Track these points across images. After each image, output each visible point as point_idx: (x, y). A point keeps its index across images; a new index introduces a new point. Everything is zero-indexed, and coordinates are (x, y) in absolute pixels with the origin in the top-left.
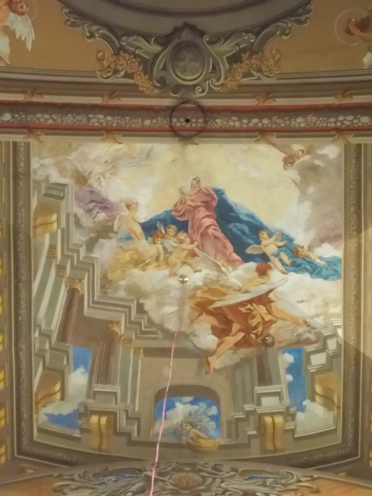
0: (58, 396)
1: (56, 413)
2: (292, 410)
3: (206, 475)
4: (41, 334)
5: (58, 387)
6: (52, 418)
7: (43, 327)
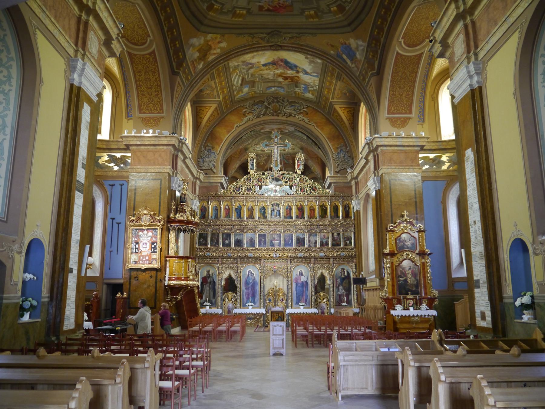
3: (280, 104)
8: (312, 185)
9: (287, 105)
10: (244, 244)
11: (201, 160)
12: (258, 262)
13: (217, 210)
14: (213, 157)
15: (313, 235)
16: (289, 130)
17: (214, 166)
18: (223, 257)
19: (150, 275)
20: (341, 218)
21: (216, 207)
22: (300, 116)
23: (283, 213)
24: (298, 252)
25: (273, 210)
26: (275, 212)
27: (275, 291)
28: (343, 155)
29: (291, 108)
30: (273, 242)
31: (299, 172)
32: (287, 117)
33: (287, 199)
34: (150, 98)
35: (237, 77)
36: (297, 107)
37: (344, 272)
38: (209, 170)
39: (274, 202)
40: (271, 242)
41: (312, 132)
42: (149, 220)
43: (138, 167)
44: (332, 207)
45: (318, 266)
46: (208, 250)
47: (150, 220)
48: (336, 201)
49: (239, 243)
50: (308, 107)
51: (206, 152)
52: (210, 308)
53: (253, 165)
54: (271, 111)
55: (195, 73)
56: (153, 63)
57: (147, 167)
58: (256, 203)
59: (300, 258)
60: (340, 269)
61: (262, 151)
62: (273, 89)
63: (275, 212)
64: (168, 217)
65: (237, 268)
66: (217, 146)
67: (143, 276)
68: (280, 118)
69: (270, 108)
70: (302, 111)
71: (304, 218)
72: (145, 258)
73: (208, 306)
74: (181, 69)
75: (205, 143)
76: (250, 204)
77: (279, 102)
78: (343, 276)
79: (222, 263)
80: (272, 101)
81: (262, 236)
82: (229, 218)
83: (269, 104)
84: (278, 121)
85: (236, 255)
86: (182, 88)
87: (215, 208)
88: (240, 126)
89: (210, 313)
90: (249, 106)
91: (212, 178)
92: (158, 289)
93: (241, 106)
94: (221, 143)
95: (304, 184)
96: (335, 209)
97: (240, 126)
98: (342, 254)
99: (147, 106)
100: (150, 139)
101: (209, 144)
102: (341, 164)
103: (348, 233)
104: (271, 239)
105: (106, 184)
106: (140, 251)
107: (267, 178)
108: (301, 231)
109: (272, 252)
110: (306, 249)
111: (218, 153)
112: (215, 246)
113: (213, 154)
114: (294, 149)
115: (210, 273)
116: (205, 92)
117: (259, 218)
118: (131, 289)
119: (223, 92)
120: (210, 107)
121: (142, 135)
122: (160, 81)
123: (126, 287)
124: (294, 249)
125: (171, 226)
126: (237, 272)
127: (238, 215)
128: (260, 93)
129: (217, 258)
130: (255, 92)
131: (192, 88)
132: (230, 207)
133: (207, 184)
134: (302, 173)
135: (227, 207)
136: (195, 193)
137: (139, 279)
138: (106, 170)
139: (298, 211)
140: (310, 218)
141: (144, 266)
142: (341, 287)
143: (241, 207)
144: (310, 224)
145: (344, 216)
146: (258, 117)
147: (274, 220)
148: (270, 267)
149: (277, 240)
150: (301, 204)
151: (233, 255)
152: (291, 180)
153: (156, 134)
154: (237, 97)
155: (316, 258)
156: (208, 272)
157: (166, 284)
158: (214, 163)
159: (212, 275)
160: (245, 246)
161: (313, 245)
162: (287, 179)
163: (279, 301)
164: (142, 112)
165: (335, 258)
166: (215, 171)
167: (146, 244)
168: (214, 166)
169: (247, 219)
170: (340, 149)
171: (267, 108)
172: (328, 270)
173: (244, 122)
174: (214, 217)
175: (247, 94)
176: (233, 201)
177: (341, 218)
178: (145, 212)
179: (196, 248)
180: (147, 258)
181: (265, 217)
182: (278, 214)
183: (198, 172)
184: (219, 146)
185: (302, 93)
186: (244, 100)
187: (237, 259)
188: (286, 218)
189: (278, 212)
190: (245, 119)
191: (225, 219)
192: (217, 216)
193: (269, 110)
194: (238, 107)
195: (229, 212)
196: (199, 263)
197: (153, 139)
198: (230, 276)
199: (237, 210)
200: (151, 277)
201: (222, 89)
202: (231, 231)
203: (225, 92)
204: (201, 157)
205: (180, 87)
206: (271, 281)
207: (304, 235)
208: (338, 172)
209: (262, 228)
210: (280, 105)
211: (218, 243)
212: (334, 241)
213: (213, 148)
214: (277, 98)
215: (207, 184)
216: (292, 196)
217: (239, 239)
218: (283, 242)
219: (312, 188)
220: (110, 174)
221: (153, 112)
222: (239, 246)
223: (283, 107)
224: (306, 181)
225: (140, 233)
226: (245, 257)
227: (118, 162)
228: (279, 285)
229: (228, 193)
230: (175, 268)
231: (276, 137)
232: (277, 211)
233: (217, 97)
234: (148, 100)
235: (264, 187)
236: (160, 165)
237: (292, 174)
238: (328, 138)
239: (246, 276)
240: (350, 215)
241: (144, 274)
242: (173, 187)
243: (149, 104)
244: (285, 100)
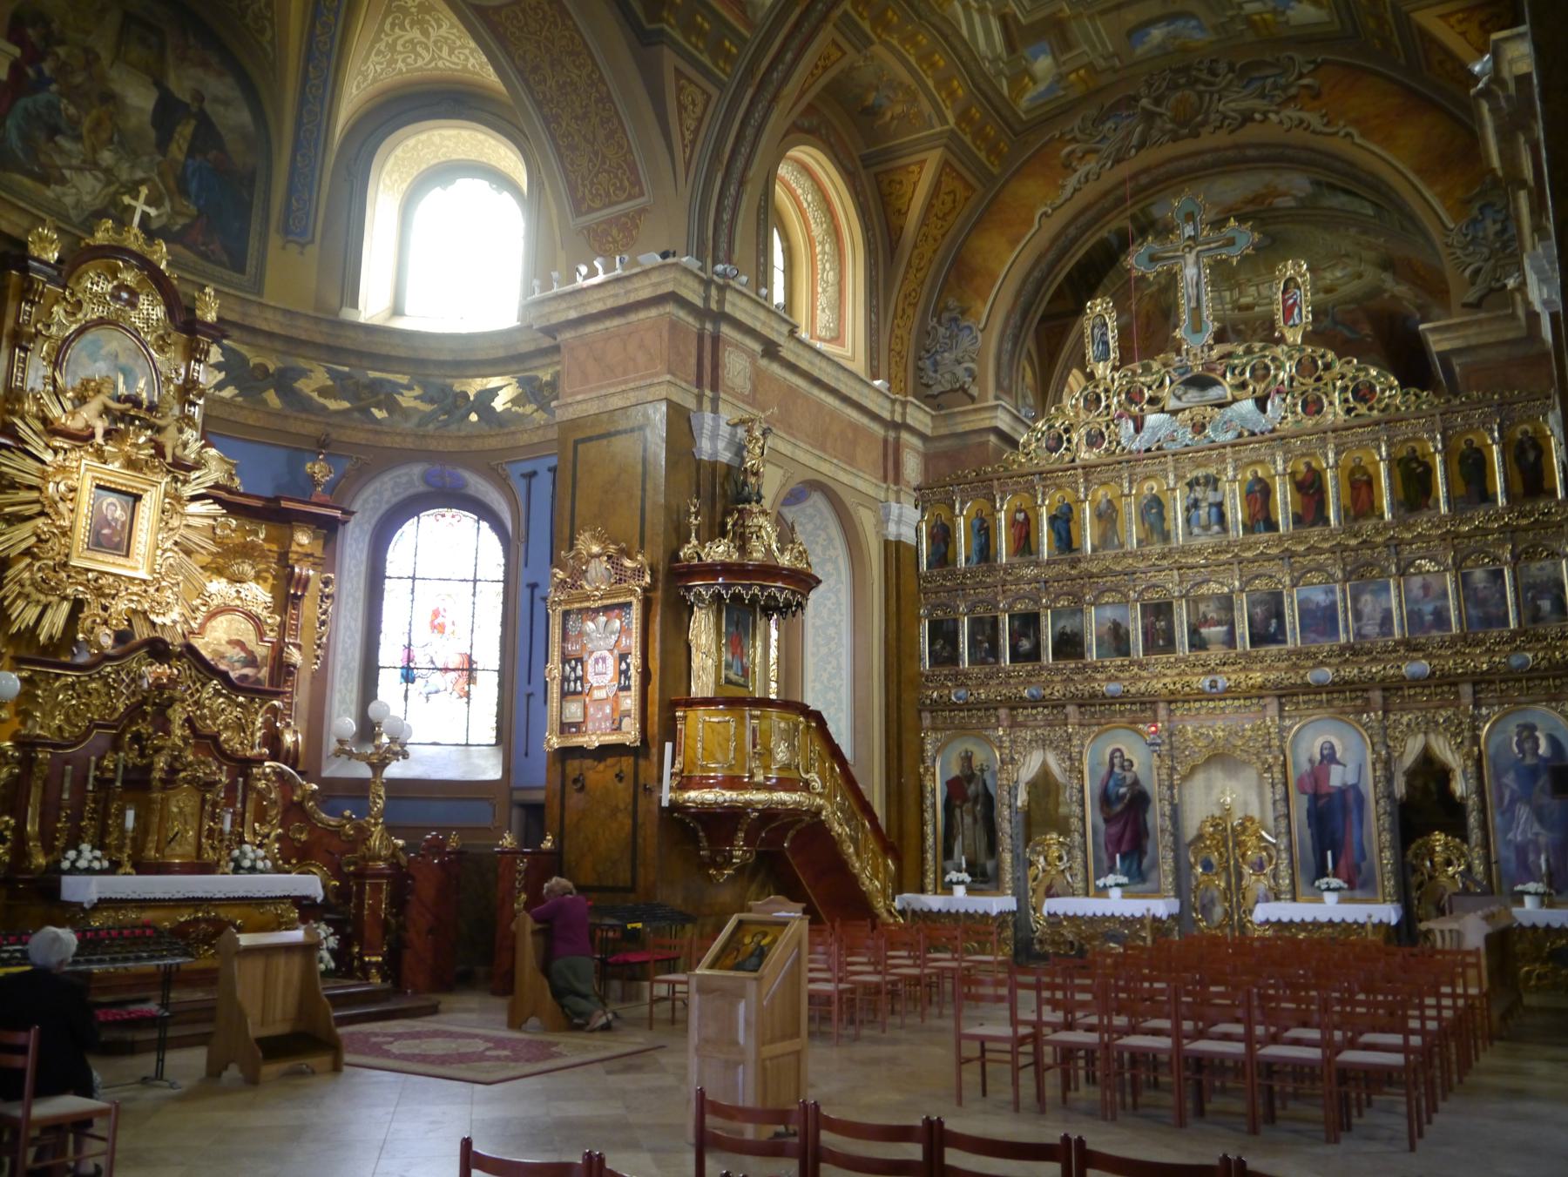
0: (1031, 84)
1: (1035, 94)
2: (1280, 9)
4: (990, 62)
5: (1027, 79)
6: (1033, 99)
7: (990, 56)
8: (1354, 379)
9: (1231, 81)
10: (1090, 650)
11: (928, 362)
12: (1149, 713)
13: (984, 531)
14: (965, 341)
16: (1295, 197)
17: (970, 372)
18: (1015, 704)
19: (617, 770)
20: (1501, 501)
21: (983, 521)
22: (1291, 112)
23: (1236, 512)
24: (1310, 663)
25: (1195, 504)
26: (1203, 512)
27: (1225, 829)
28: (1498, 226)
29: (1245, 92)
30: (1204, 631)
31: (1294, 336)
32: (1232, 132)
33: (1246, 454)
34: (596, 154)
35: (977, 18)
36: (1270, 80)
37: (1536, 741)
38: (955, 391)
39: (1195, 474)
40: (1194, 631)
41: (1352, 164)
42: (606, 573)
43: (579, 397)
44: (1456, 458)
45: (1405, 720)
46: (960, 679)
47: (610, 576)
48: (1471, 429)
49: (1069, 645)
50: (1318, 66)
51: (942, 330)
52: (970, 890)
53: (1106, 343)
54: (1169, 126)
55: (750, 25)
56: (559, 20)
57: (603, 392)
58: (1126, 485)
59: (1318, 689)
60: (1512, 729)
61: (1241, 308)
62: (1157, 34)
63: (1203, 512)
64: (675, 557)
65: (1070, 740)
66: (979, 304)
67: (600, 775)
68: (1207, 140)
69: (1161, 115)
70: (1293, 91)
71: (1326, 521)
72: (602, 709)
73: (958, 883)
74: (665, 14)
75: (939, 296)
76: (1101, 493)
77: (1197, 80)
78: (1529, 761)
79: (1014, 724)
80: (1168, 88)
81: (1159, 611)
82: (1031, 553)
83: (1157, 101)
84: (1208, 158)
85: (1058, 691)
86: (704, 92)
87: (977, 523)
88: (1054, 210)
89: (962, 910)
90: (1082, 131)
91: (959, 419)
92: (640, 821)
93: (1052, 139)
94: (992, 287)
95: (1319, 379)
96: (1472, 468)
97: (1054, 210)
98: (1515, 661)
99: (592, 184)
100: (596, 295)
101: (952, 302)
102: (1488, 266)
104: (1193, 620)
105: (515, 472)
106: (587, 686)
107: (1161, 384)
108: (1316, 578)
109: (1200, 670)
110: (1343, 649)
111: (981, 326)
112: (983, 662)
113: (966, 332)
114: (1360, 276)
115: (976, 763)
116: (889, 115)
117: (1139, 542)
118: (567, 821)
119: (952, 94)
120: (922, 163)
121: (581, 282)
122: (605, 84)
123: (553, 813)
124: (1290, 653)
125: (689, 589)
126: (1070, 758)
127: (1060, 539)
128: (1115, 70)
129: (989, 706)
130: (1090, 68)
131: (771, 89)
132: (1031, 514)
133: (947, 443)
134: (1307, 338)
135: (1020, 517)
136: (897, 479)
137: (588, 783)
138: (513, 428)
139: (1298, 497)
140: (1356, 519)
141: (592, 741)
142: (1523, 812)
143: (1070, 509)
144: (1353, 542)
145: (1518, 488)
146: (1117, 161)
147: (1197, 543)
148: (1194, 731)
149: (1219, 623)
150: (1308, 465)
151: (1048, 691)
152: (1260, 373)
153: (615, 269)
154: (1024, 103)
155: (1392, 687)
156: (967, 758)
157: (665, 803)
158: (971, 365)
159: (982, 770)
160: (1092, 656)
161: (1371, 629)
162: (1242, 373)
163: (1247, 870)
164: (584, 208)
165: (1480, 681)
166: (974, 391)
167: (604, 660)
168: (970, 372)
169: (1094, 549)
170: (1477, 205)
171: (1149, 117)
172: (1455, 735)
173: (1068, 191)
174: (975, 559)
175: (1058, 82)
176: (1039, 489)
177: (1501, 501)
178: (595, 549)
179: (921, 674)
180: (608, 710)
181: (1166, 537)
182: (1214, 518)
183: (893, 401)
184: (985, 302)
185: (1274, 11)
186: (1056, 112)
187: (1064, 707)
188: (1249, 528)
189: (1214, 510)
190: (1072, 182)
191: (1016, 560)
192: (985, 552)
193: (1158, 122)
194: (1045, 144)
195: (1028, 534)
196: (935, 729)
197: (611, 290)
198: (1045, 771)
199: (1058, 523)
200: (619, 777)
201: (943, 83)
202: (1037, 601)
203: (960, 92)
204: (928, 351)
205: (691, 88)
206: (1209, 788)
207: (1332, 591)
208: (1477, 305)
209: (1154, 580)
210: (1200, 95)
211: (994, 651)
213: (963, 312)
214: (1185, 70)
215: (947, 443)
216: (1268, 435)
217: (1068, 630)
218: (1243, 629)
219: (1355, 392)
220: (524, 439)
221: (614, 198)
222: (1068, 656)
223: (1216, 96)
224: (1328, 367)
225: (590, 626)
226: (1093, 696)
227: (545, 397)
228: (1246, 804)
229: (1021, 464)
230: (703, 741)
231: (1190, 217)
232: (1211, 505)
233: (935, 121)
234: (590, 160)
235: (1152, 419)
236: (642, 378)
237: (1263, 349)
238: (1418, 172)
239: (1104, 770)
240: (1546, 485)
241: (601, 767)
242: (700, 449)
243: (596, 176)
244: (1222, 67)
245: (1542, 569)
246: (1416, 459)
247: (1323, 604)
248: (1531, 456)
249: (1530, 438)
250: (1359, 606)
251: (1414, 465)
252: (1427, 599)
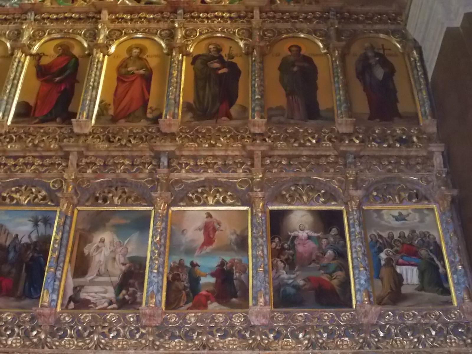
15: (114, 221)
103: (406, 208)
139: (36, 84)
140: (114, 120)
207: (48, 222)
212: (291, 264)
245: (400, 218)
246: (220, 59)
247: (25, 240)
248: (380, 73)
249: (377, 54)
250: (86, 251)
251: (216, 65)
252: (209, 249)
